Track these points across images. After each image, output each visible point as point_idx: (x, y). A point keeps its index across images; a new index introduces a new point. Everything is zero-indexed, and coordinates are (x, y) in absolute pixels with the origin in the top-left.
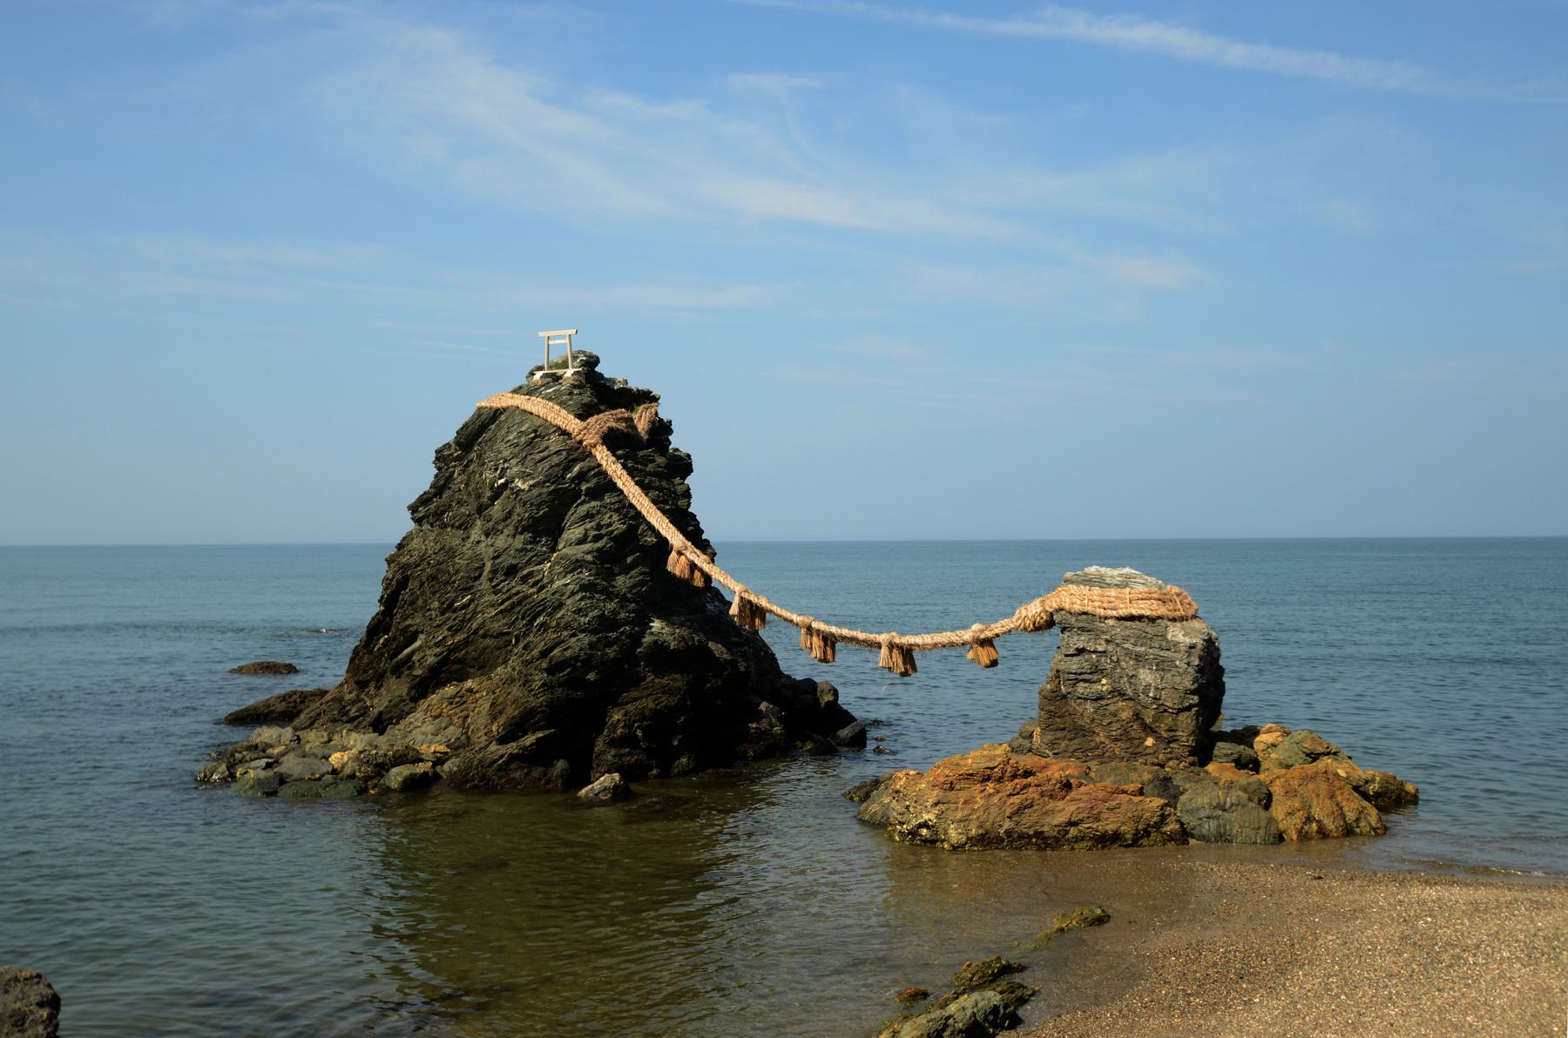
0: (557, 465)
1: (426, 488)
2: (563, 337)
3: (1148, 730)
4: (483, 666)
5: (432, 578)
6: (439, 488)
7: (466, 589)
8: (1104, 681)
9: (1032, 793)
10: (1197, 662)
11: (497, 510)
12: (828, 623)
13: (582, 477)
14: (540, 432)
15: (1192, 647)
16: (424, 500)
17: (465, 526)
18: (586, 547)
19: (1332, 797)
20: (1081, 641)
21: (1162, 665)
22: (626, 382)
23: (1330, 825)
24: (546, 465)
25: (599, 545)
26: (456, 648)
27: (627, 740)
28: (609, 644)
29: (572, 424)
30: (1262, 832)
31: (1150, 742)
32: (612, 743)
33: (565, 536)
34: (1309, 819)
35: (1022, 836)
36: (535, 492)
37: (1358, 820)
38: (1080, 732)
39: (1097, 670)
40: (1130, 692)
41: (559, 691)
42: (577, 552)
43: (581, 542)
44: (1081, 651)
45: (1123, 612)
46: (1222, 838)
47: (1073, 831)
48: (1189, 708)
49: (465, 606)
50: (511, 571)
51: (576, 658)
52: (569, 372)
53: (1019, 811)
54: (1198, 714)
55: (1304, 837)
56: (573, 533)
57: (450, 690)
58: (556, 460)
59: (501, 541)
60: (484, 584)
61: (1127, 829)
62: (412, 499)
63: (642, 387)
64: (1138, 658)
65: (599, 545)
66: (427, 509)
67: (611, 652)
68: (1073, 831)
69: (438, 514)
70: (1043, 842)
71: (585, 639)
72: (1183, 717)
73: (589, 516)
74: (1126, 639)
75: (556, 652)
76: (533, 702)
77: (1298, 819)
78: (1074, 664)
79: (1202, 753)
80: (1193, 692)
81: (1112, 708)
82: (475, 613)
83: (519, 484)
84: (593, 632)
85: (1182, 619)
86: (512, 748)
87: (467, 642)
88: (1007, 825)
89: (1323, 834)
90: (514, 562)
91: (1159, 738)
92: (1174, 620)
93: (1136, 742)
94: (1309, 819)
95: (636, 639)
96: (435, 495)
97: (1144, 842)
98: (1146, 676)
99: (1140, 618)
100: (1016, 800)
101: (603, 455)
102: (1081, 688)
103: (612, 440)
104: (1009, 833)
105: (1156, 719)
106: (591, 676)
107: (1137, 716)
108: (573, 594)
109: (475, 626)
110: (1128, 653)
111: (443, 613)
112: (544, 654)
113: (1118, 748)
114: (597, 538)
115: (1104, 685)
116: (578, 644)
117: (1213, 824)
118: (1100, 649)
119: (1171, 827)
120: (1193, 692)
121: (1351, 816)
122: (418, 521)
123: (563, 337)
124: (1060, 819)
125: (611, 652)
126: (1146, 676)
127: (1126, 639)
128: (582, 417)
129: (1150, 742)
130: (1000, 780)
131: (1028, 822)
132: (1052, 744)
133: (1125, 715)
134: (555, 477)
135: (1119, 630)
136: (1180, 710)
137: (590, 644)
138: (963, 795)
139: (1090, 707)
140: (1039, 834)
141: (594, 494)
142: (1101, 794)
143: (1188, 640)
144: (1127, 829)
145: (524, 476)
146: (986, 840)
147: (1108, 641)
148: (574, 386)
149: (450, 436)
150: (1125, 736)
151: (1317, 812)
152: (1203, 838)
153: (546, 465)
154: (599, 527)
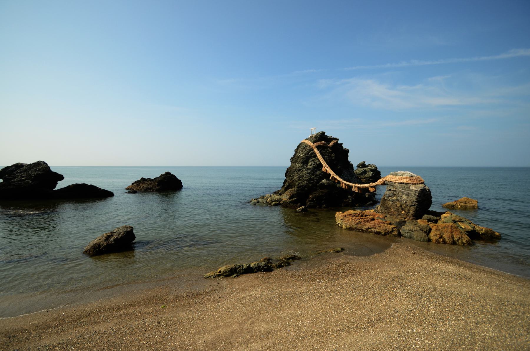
3: (403, 209)
6: (294, 156)
9: (362, 220)
12: (347, 181)
13: (312, 154)
15: (416, 191)
16: (292, 158)
19: (452, 232)
20: (390, 188)
21: (408, 195)
23: (447, 240)
27: (312, 201)
29: (311, 144)
30: (422, 239)
32: (309, 201)
34: (441, 237)
35: (358, 229)
37: (458, 240)
38: (388, 208)
44: (390, 190)
45: (399, 182)
46: (411, 238)
47: (369, 230)
48: (414, 205)
50: (300, 170)
53: (357, 224)
54: (417, 207)
55: (437, 242)
56: (310, 164)
59: (299, 165)
61: (383, 232)
63: (335, 137)
64: (403, 192)
66: (293, 160)
68: (369, 230)
70: (362, 231)
71: (305, 182)
72: (412, 207)
73: (313, 161)
74: (400, 188)
76: (294, 193)
77: (437, 237)
78: (388, 193)
79: (418, 216)
80: (416, 202)
85: (415, 184)
88: (355, 226)
89: (444, 242)
91: (405, 212)
92: (413, 184)
94: (441, 237)
97: (387, 235)
98: (404, 197)
99: (403, 183)
100: (357, 221)
101: (316, 150)
103: (318, 147)
104: (355, 228)
105: (405, 207)
107: (401, 206)
110: (400, 191)
113: (395, 213)
117: (409, 234)
119: (395, 233)
120: (416, 202)
121: (456, 239)
124: (367, 227)
127: (400, 188)
128: (313, 143)
129: (403, 212)
130: (357, 216)
131: (360, 226)
132: (381, 210)
133: (398, 205)
134: (307, 154)
135: (398, 186)
136: (411, 206)
138: (347, 219)
139: (391, 203)
140: (362, 229)
142: (377, 223)
143: (415, 189)
144: (383, 232)
145: (302, 154)
146: (350, 229)
150: (397, 210)
151: (444, 236)
152: (405, 237)
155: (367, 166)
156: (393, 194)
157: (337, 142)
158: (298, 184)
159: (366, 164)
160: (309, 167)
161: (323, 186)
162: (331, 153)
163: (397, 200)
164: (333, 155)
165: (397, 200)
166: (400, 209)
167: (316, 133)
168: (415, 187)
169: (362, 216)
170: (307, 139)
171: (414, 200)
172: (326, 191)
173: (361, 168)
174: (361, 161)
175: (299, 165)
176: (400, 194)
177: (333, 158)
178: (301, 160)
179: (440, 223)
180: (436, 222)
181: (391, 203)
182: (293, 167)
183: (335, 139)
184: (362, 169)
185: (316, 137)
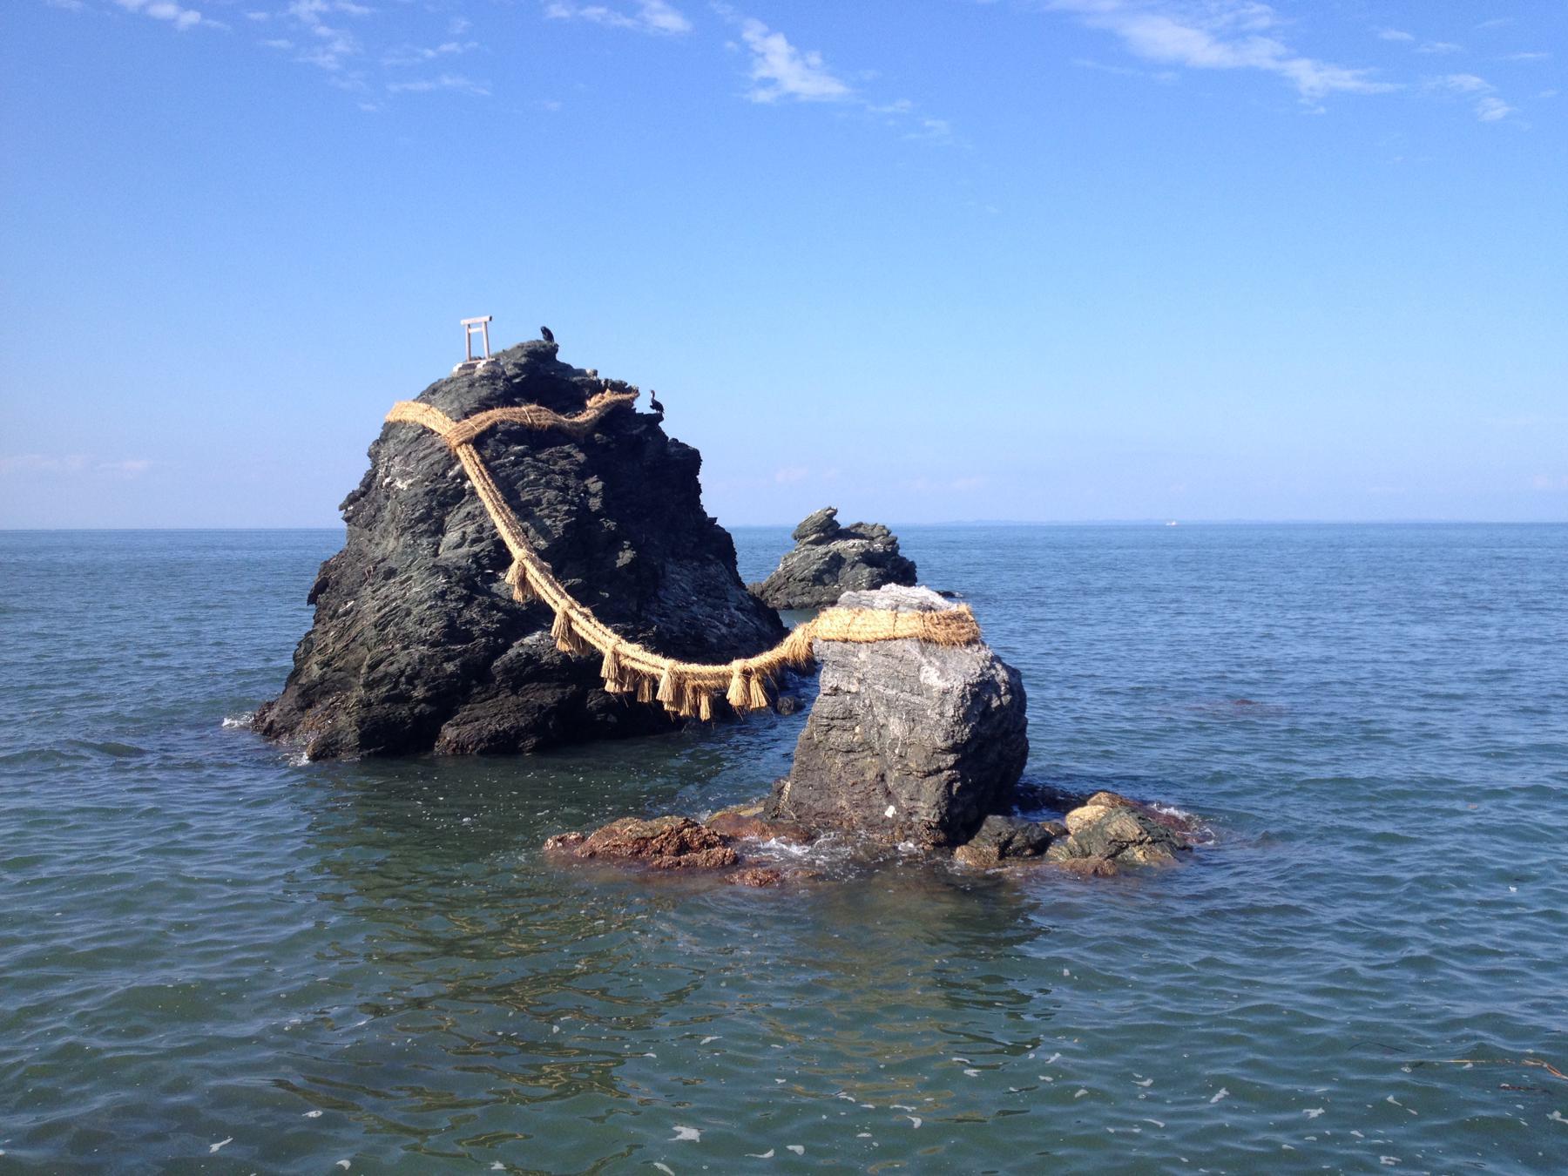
0: (438, 462)
1: (356, 487)
2: (478, 325)
7: (351, 594)
8: (857, 729)
10: (951, 712)
11: (387, 514)
15: (945, 693)
16: (353, 499)
18: (464, 550)
21: (913, 717)
22: (595, 373)
24: (427, 462)
25: (476, 548)
28: (448, 659)
33: (445, 540)
36: (412, 493)
40: (877, 746)
41: (377, 710)
48: (939, 771)
49: (347, 613)
56: (452, 537)
58: (437, 457)
62: (342, 499)
63: (615, 378)
64: (889, 704)
65: (476, 548)
67: (450, 667)
75: (382, 668)
81: (859, 764)
82: (354, 622)
84: (433, 645)
90: (395, 566)
91: (899, 808)
93: (875, 811)
96: (363, 494)
98: (896, 728)
105: (901, 783)
106: (419, 693)
108: (421, 602)
109: (353, 633)
111: (331, 618)
114: (474, 541)
118: (854, 689)
122: (347, 520)
123: (478, 325)
125: (450, 667)
126: (896, 728)
127: (877, 678)
137: (421, 661)
139: (839, 760)
145: (404, 475)
147: (860, 681)
148: (482, 378)
153: (427, 462)
154: (481, 529)
155: (847, 534)
156: (849, 715)
157: (630, 402)
158: (372, 668)
159: (844, 520)
160: (447, 554)
162: (582, 474)
163: (866, 745)
164: (595, 484)
165: (866, 745)
166: (878, 798)
167: (497, 349)
168: (943, 673)
169: (683, 847)
171: (940, 743)
172: (548, 697)
173: (817, 542)
174: (814, 509)
175: (390, 545)
176: (880, 710)
177: (595, 504)
178: (403, 513)
179: (1058, 853)
180: (1040, 848)
181: (839, 760)
182: (361, 555)
183: (619, 387)
184: (821, 549)
185: (492, 377)
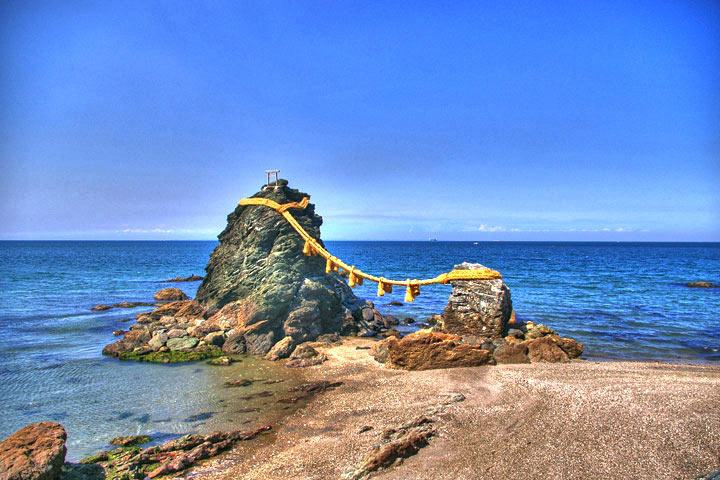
3: (484, 324)
4: (243, 295)
5: (226, 263)
11: (249, 238)
13: (280, 226)
14: (263, 210)
16: (223, 234)
17: (238, 244)
21: (489, 300)
26: (234, 288)
31: (484, 328)
32: (290, 325)
38: (460, 324)
39: (465, 301)
42: (277, 254)
43: (279, 250)
44: (459, 295)
50: (254, 261)
51: (276, 294)
52: (276, 187)
57: (232, 304)
59: (250, 250)
60: (244, 265)
64: (480, 297)
67: (290, 291)
69: (228, 240)
72: (497, 319)
73: (282, 241)
74: (476, 290)
78: (457, 299)
79: (504, 333)
83: (257, 228)
86: (253, 327)
87: (237, 287)
95: (299, 287)
98: (483, 304)
101: (288, 216)
102: (459, 308)
106: (283, 300)
107: (480, 319)
112: (265, 292)
114: (285, 249)
115: (468, 307)
116: (278, 288)
125: (290, 291)
129: (484, 328)
132: (449, 328)
139: (463, 315)
141: (284, 233)
145: (259, 226)
149: (233, 210)
150: (475, 325)
156: (465, 301)
161: (309, 294)
165: (473, 310)
170: (257, 196)
176: (477, 300)
178: (258, 239)
